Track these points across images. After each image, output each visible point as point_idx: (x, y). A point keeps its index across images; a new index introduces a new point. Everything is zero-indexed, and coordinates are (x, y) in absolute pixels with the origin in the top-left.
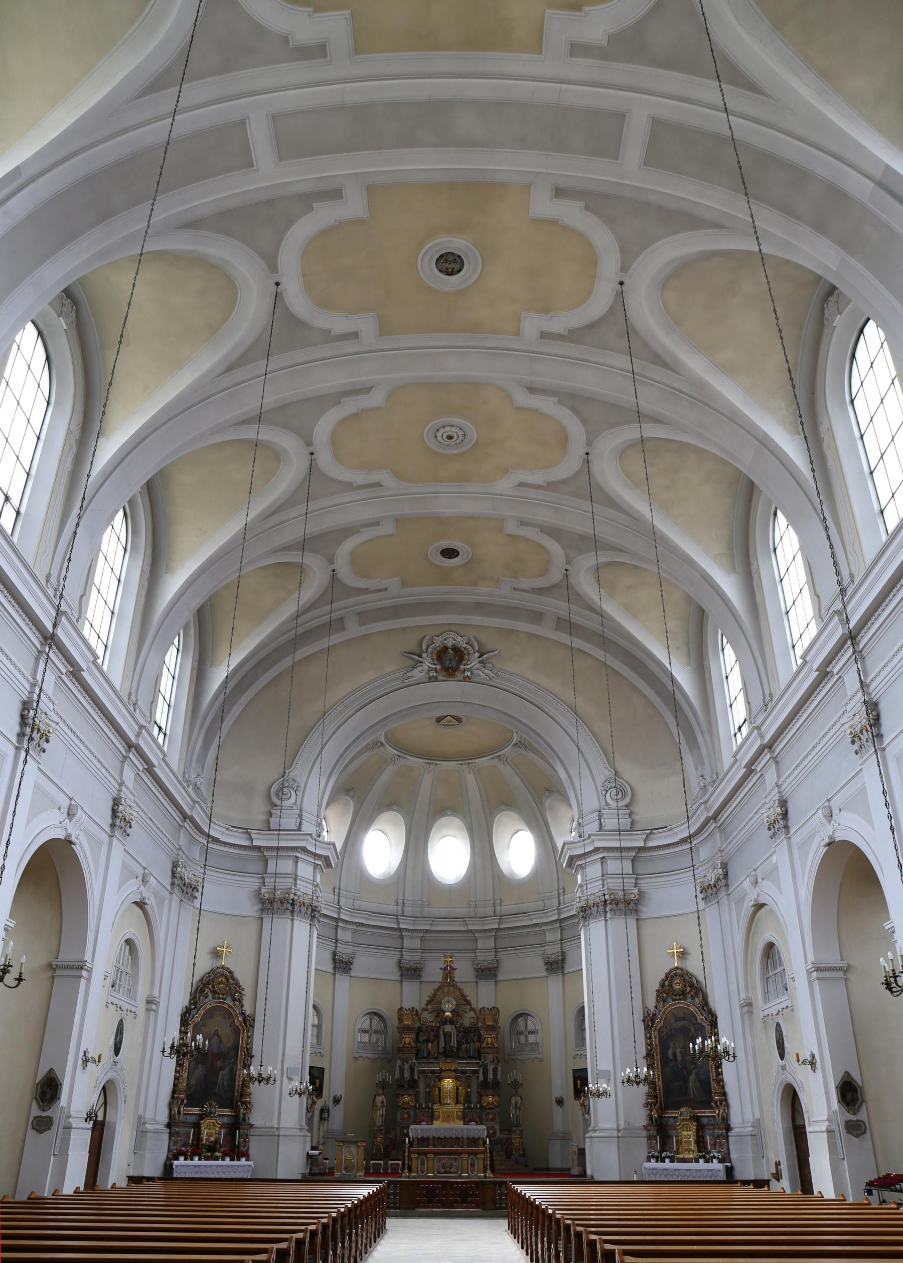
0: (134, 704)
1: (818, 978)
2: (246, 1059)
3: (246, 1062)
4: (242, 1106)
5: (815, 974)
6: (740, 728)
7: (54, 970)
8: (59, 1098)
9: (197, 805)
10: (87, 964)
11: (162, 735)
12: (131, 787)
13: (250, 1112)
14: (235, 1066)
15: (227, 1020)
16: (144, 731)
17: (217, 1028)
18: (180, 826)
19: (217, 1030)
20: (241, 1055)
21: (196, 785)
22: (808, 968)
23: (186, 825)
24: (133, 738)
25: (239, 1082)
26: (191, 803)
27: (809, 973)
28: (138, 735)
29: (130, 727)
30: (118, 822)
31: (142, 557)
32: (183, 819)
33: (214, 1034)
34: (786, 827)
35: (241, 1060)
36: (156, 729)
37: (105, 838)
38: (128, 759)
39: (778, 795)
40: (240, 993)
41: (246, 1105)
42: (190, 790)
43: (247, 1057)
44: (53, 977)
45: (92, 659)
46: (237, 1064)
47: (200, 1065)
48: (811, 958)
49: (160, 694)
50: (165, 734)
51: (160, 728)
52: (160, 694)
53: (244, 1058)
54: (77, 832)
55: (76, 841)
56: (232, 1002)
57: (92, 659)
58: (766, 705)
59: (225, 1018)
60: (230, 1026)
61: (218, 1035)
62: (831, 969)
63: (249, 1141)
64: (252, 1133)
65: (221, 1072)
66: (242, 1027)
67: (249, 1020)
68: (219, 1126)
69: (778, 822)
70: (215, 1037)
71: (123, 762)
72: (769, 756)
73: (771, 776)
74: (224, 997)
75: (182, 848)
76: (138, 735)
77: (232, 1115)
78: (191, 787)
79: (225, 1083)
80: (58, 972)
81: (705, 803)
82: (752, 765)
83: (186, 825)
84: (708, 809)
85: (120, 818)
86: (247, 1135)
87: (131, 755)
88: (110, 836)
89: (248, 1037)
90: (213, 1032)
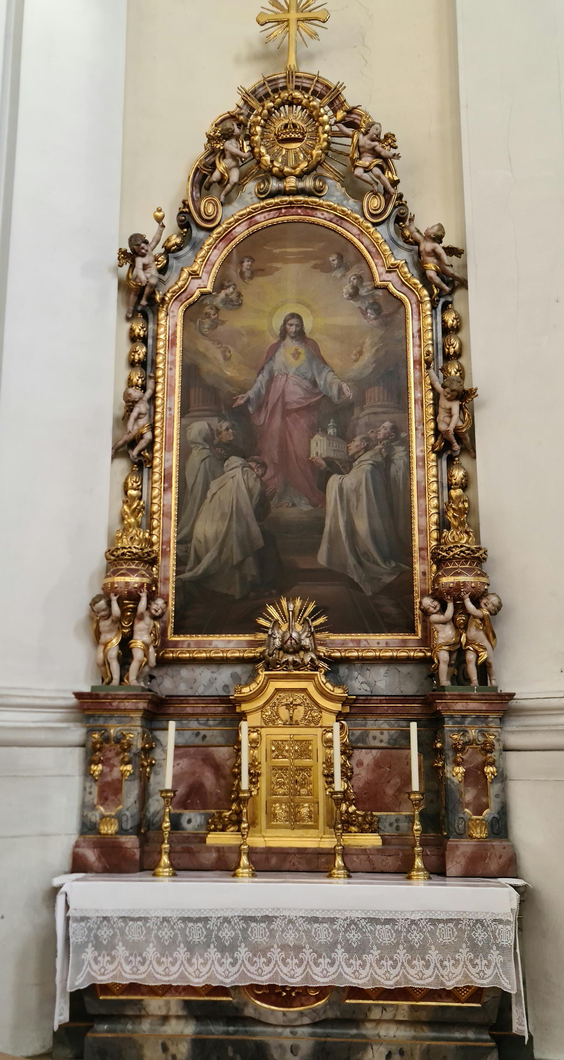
2: (442, 415)
3: (442, 427)
4: (443, 609)
13: (491, 635)
14: (399, 451)
15: (338, 274)
17: (297, 309)
19: (293, 316)
20: (420, 402)
25: (425, 513)
33: (284, 333)
35: (421, 422)
40: (377, 155)
41: (460, 608)
43: (444, 403)
46: (406, 443)
47: (235, 461)
53: (436, 414)
56: (351, 201)
59: (326, 268)
60: (354, 295)
61: (300, 335)
63: (502, 777)
64: (513, 740)
65: (334, 481)
66: (412, 289)
67: (434, 254)
68: (337, 707)
70: (291, 345)
74: (308, 183)
77: (408, 660)
79: (362, 526)
86: (487, 749)
89: (446, 331)
90: (277, 323)
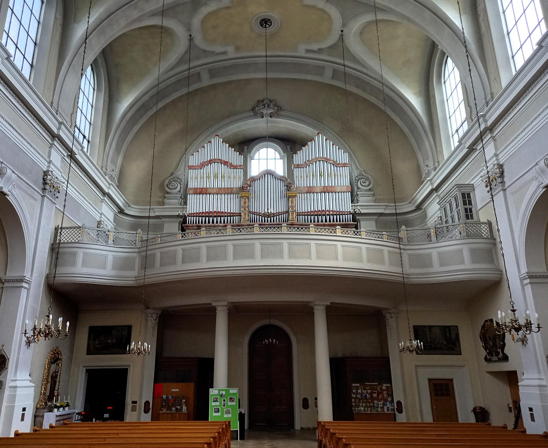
0: (57, 111)
1: (530, 283)
5: (528, 281)
6: (457, 131)
7: (3, 283)
8: (7, 368)
9: (111, 186)
10: (26, 278)
11: (86, 142)
12: (59, 166)
16: (62, 126)
18: (102, 199)
21: (112, 176)
22: (521, 276)
23: (106, 199)
24: (55, 130)
26: (107, 184)
27: (522, 280)
28: (59, 129)
29: (54, 124)
30: (47, 187)
31: (55, 6)
32: (103, 195)
34: (503, 182)
36: (81, 137)
37: (39, 197)
38: (54, 146)
39: (499, 158)
42: (107, 177)
44: (3, 288)
45: (6, 56)
48: (524, 270)
49: (78, 109)
50: (88, 142)
51: (84, 137)
52: (78, 109)
54: (10, 187)
55: (8, 193)
57: (6, 56)
58: (487, 103)
62: (540, 277)
69: (496, 180)
71: (51, 147)
72: (489, 136)
73: (490, 151)
75: (104, 213)
76: (59, 129)
78: (107, 176)
80: (6, 285)
81: (430, 180)
82: (474, 145)
83: (106, 199)
84: (432, 184)
85: (49, 184)
87: (55, 143)
88: (43, 196)
